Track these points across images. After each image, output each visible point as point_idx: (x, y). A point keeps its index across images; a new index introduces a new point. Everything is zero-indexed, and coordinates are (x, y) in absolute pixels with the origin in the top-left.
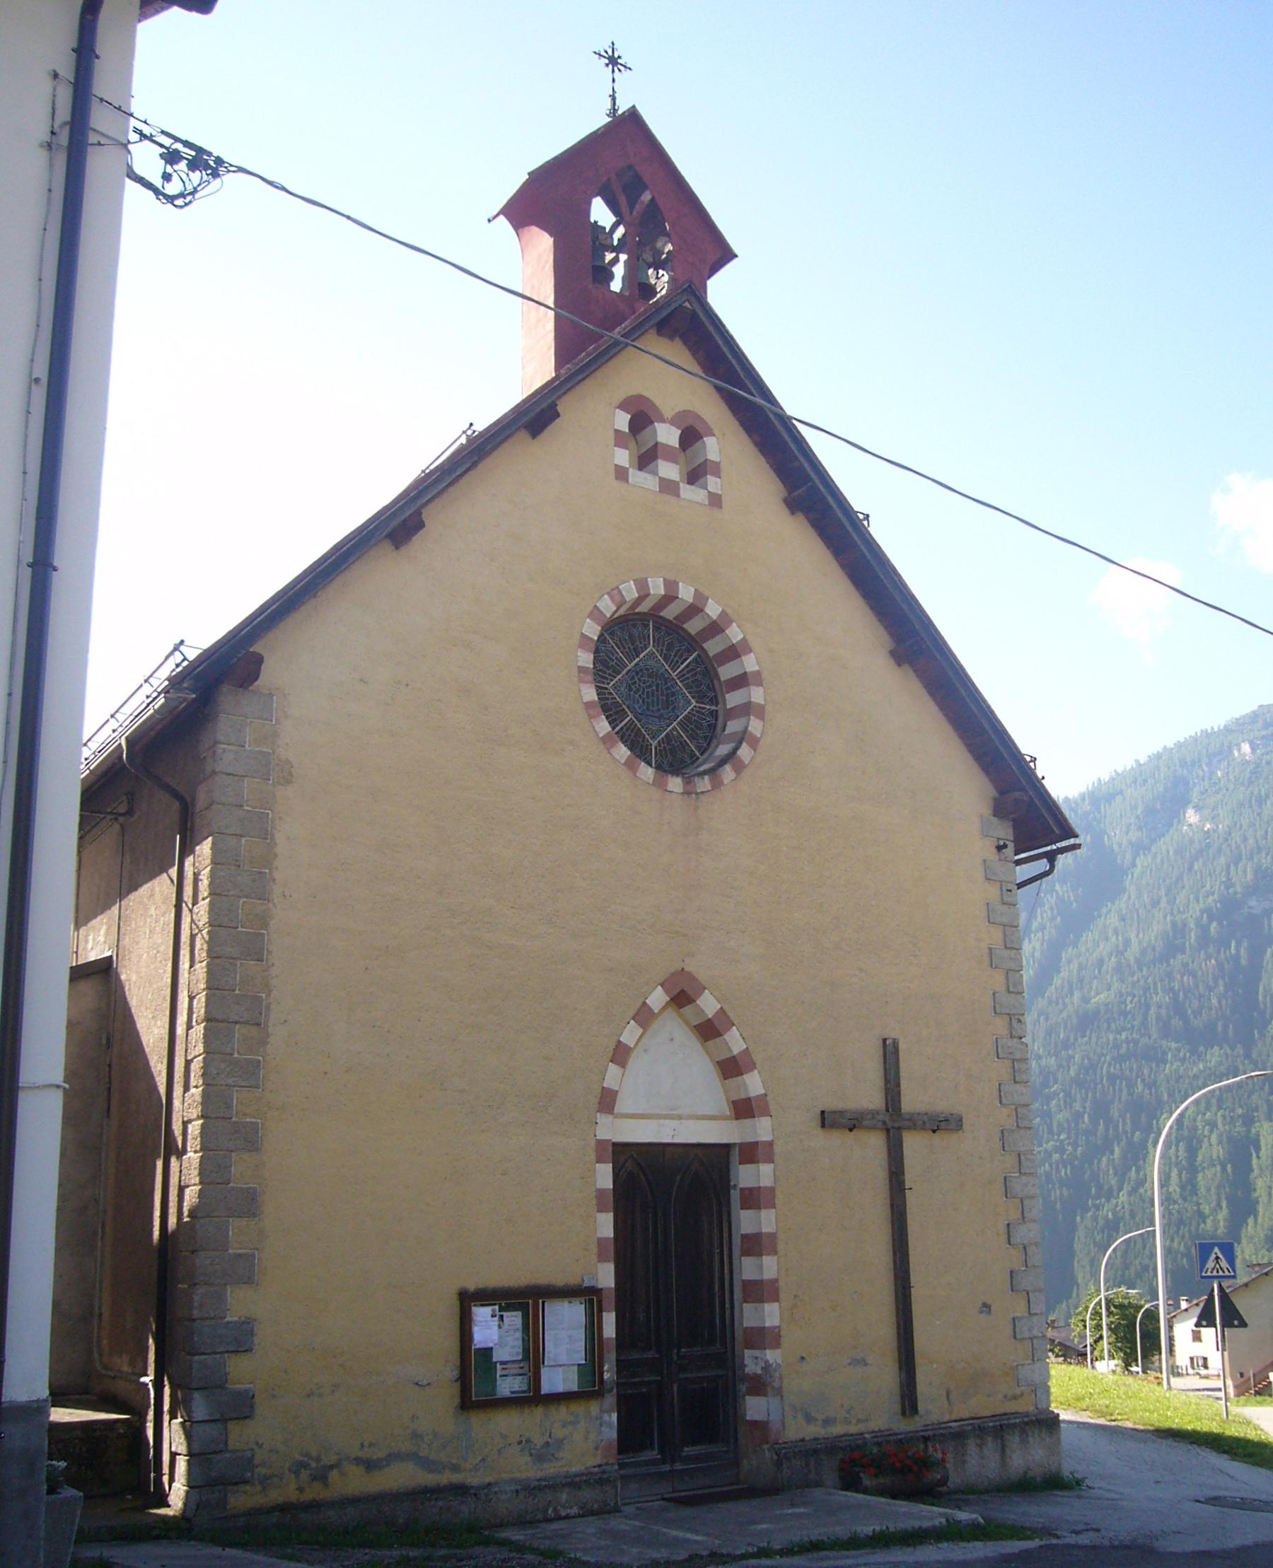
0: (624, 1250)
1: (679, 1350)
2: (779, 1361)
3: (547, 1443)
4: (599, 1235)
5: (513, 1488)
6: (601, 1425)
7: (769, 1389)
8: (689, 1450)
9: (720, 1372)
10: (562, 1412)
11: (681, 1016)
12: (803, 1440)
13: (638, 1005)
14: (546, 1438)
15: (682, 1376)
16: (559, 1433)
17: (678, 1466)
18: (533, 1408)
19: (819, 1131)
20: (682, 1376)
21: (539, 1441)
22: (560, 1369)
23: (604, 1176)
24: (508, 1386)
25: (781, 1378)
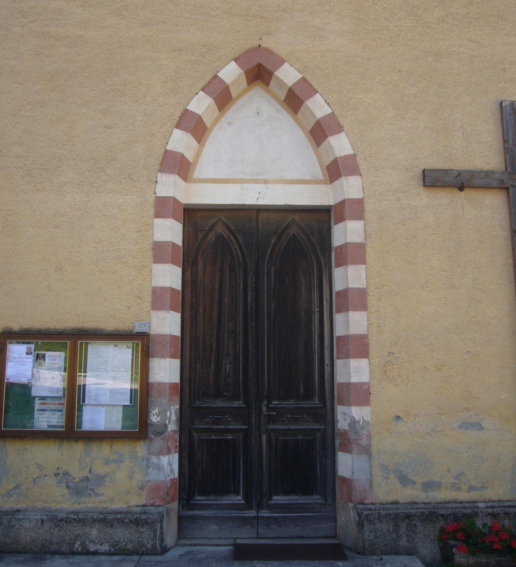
0: (190, 300)
1: (269, 402)
2: (368, 418)
3: (87, 479)
4: (154, 284)
5: (39, 517)
6: (148, 466)
7: (354, 447)
8: (279, 499)
9: (317, 426)
10: (105, 450)
11: (269, 92)
12: (396, 503)
13: (209, 78)
14: (86, 474)
15: (271, 427)
16: (100, 469)
17: (264, 513)
18: (73, 444)
19: (422, 191)
20: (271, 427)
21: (77, 474)
22: (104, 409)
23: (170, 231)
24: (46, 419)
25: (369, 437)
